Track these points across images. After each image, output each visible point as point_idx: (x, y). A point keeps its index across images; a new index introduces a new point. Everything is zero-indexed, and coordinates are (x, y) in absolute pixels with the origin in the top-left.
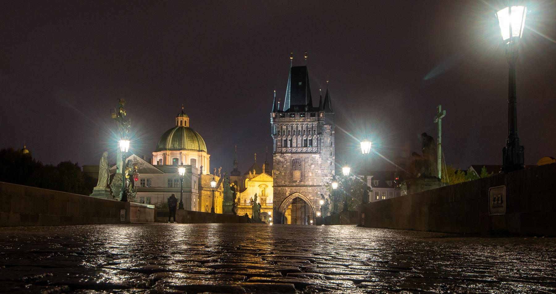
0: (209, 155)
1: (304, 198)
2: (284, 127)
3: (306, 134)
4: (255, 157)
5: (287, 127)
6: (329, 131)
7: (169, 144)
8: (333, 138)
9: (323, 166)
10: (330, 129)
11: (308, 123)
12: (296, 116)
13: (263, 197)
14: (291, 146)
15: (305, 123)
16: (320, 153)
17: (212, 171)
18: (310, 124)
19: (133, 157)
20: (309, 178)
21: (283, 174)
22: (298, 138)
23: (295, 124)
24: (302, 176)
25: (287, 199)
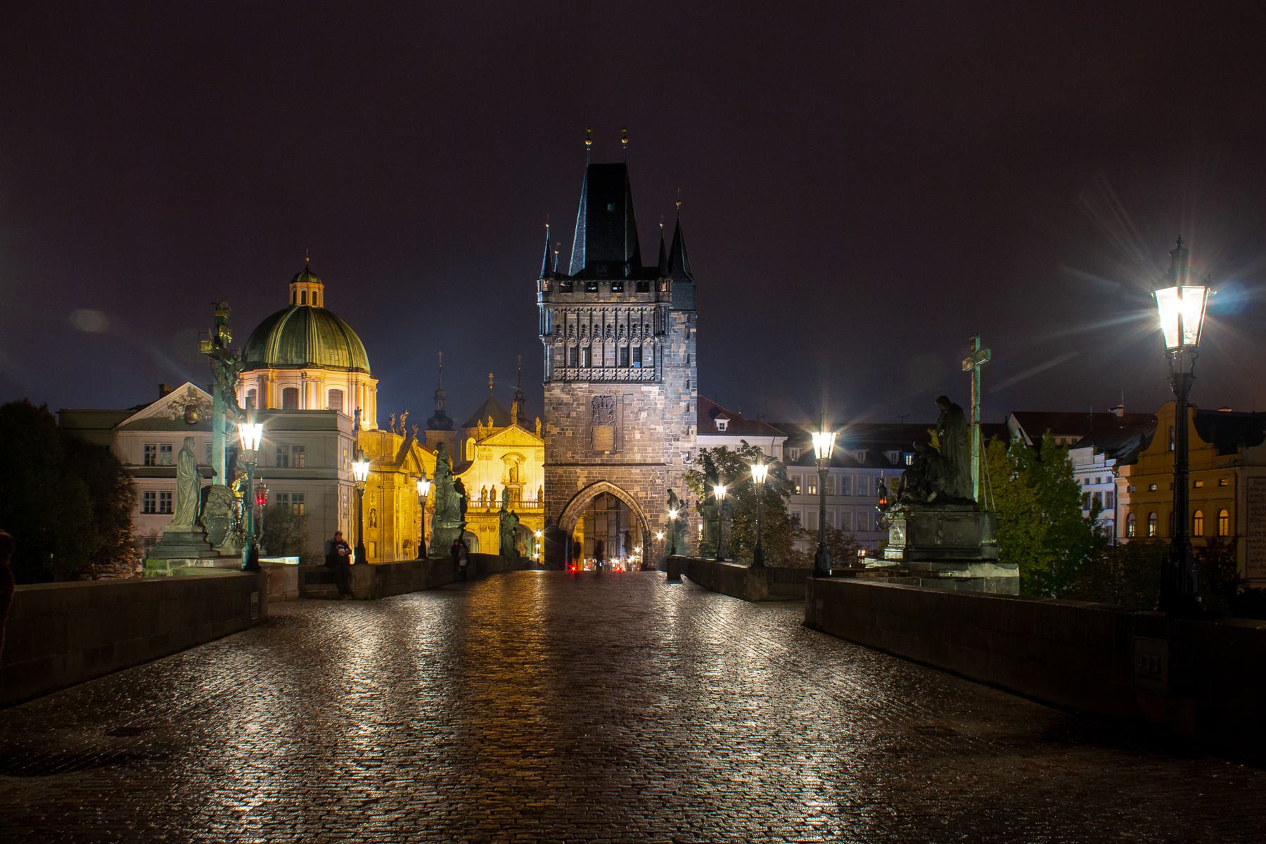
1: (622, 494)
2: (572, 317)
3: (627, 335)
4: (491, 383)
5: (578, 315)
6: (684, 326)
7: (274, 354)
8: (693, 344)
9: (668, 416)
10: (684, 323)
11: (631, 308)
12: (600, 288)
14: (589, 364)
16: (661, 382)
18: (636, 308)
21: (569, 434)
23: (598, 310)
24: (616, 438)
25: (579, 496)
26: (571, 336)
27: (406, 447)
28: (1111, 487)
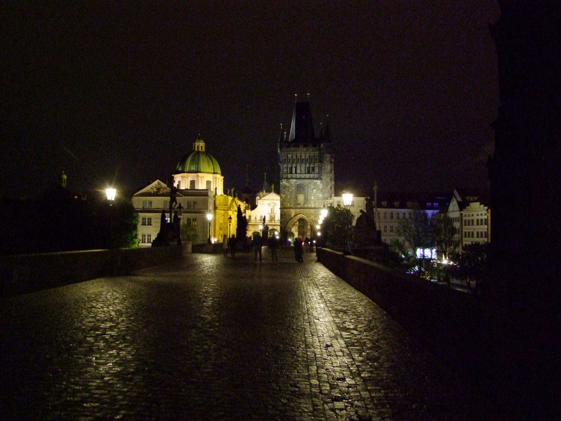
0: (223, 177)
2: (290, 156)
7: (187, 169)
8: (333, 165)
13: (272, 215)
14: (296, 173)
15: (308, 152)
17: (225, 192)
18: (312, 153)
19: (157, 182)
20: (312, 201)
21: (289, 197)
22: (302, 165)
23: (299, 153)
24: (305, 199)
25: (292, 219)
26: (289, 162)
27: (233, 200)
28: (486, 217)
